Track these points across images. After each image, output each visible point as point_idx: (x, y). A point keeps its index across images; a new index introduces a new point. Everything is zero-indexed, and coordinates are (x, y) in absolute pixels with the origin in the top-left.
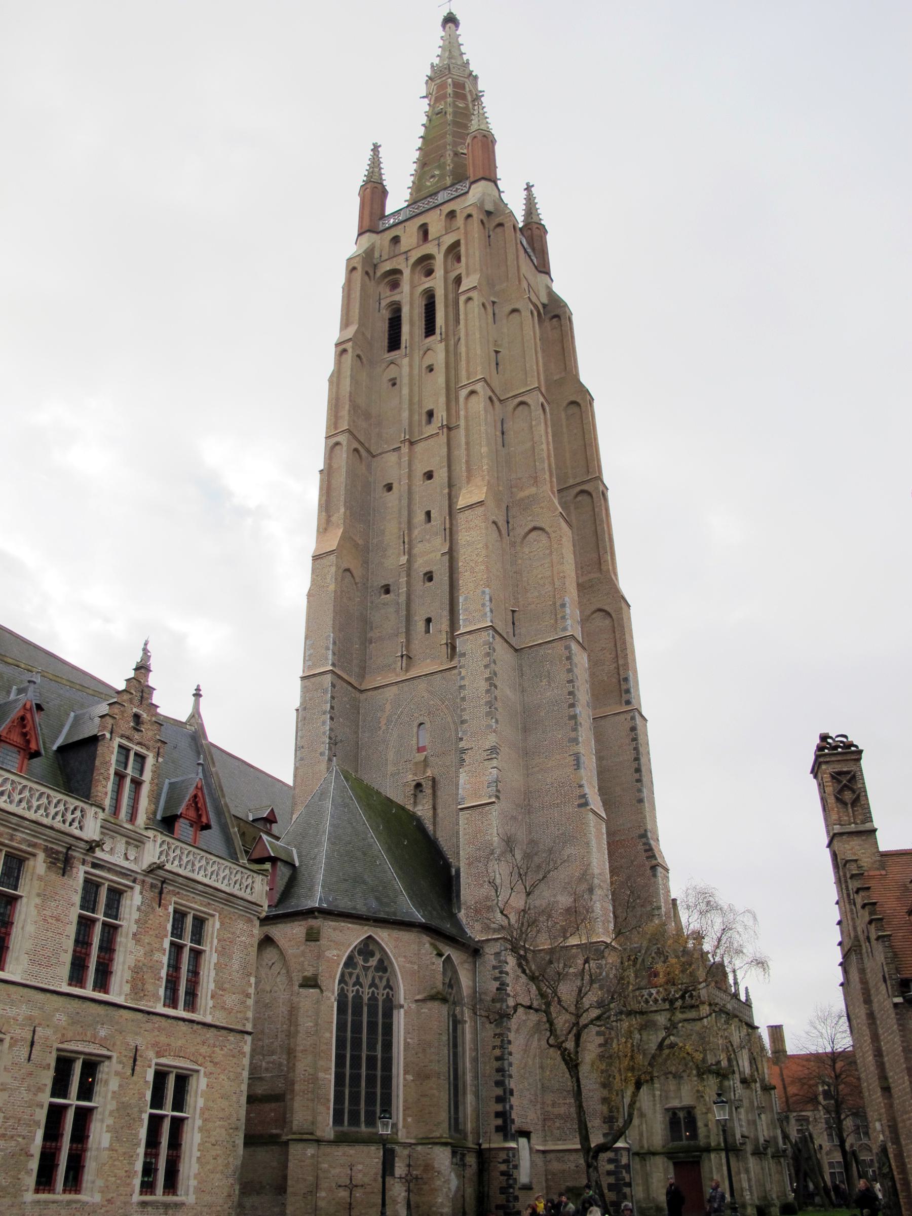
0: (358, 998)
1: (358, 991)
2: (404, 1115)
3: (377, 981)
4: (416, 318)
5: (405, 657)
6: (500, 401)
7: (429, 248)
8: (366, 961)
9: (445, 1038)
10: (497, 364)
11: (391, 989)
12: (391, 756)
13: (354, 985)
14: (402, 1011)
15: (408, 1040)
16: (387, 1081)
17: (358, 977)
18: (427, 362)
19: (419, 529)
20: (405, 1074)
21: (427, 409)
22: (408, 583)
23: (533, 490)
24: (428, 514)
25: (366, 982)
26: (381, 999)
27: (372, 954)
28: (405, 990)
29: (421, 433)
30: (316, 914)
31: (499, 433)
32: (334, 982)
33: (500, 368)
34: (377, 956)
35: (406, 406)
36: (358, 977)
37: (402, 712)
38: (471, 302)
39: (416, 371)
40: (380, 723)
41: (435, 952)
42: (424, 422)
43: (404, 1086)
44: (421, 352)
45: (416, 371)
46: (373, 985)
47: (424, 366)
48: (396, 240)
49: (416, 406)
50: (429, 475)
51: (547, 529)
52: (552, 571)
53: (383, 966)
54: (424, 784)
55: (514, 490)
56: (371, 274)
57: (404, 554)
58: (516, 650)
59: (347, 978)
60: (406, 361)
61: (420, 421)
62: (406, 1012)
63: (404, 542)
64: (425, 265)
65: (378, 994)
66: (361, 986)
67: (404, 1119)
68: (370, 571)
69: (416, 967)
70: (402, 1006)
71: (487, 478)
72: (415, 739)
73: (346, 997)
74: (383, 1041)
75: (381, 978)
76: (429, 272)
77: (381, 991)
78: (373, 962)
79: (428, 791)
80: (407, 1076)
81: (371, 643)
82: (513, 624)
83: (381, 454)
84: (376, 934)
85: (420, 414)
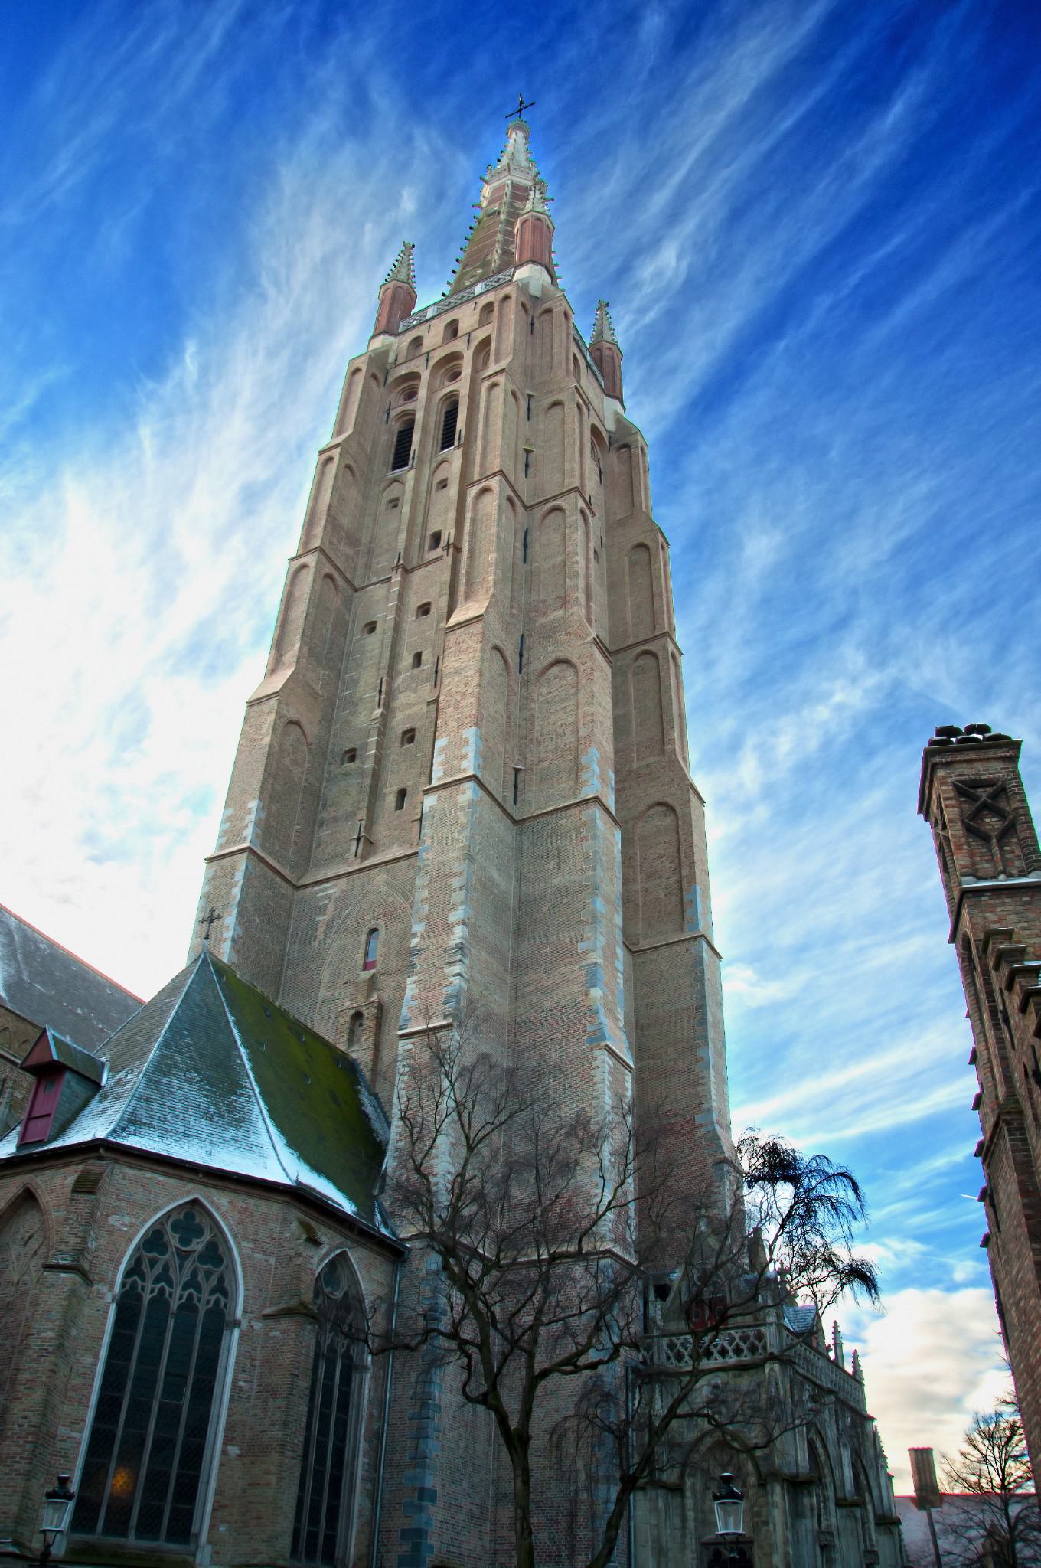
0: (160, 1302)
1: (162, 1291)
2: (213, 1517)
3: (201, 1278)
4: (432, 425)
5: (362, 840)
6: (526, 508)
7: (458, 345)
8: (186, 1241)
9: (304, 1383)
10: (527, 466)
11: (225, 1294)
12: (326, 976)
13: (157, 1280)
14: (236, 1332)
15: (241, 1384)
16: (194, 1455)
17: (166, 1268)
18: (439, 477)
19: (403, 675)
20: (225, 1444)
21: (433, 531)
22: (380, 745)
23: (560, 613)
24: (418, 657)
25: (180, 1277)
26: (202, 1308)
27: (199, 1233)
28: (246, 1297)
29: (421, 557)
30: (102, 1151)
31: (519, 545)
32: (117, 1268)
33: (531, 470)
34: (207, 1237)
35: (404, 526)
36: (166, 1268)
37: (348, 915)
38: (496, 388)
39: (424, 488)
40: (317, 930)
41: (304, 1237)
42: (427, 547)
43: (222, 1465)
44: (434, 465)
45: (424, 488)
46: (192, 1283)
47: (435, 482)
48: (417, 342)
49: (419, 528)
50: (425, 609)
51: (574, 660)
52: (577, 715)
53: (215, 1254)
54: (365, 1013)
55: (533, 614)
56: (381, 378)
57: (379, 706)
58: (515, 822)
59: (145, 1266)
60: (411, 474)
61: (422, 546)
62: (242, 1337)
63: (380, 692)
64: (450, 365)
65: (199, 1300)
66: (170, 1283)
67: (212, 1527)
68: (332, 733)
69: (272, 1260)
70: (237, 1324)
71: (492, 590)
72: (362, 951)
73: (139, 1298)
74: (196, 1381)
75: (208, 1275)
76: (455, 376)
77: (205, 1296)
78: (198, 1245)
79: (369, 1023)
80: (230, 1448)
81: (321, 825)
82: (516, 787)
83: (363, 588)
84: (207, 1198)
85: (423, 537)
